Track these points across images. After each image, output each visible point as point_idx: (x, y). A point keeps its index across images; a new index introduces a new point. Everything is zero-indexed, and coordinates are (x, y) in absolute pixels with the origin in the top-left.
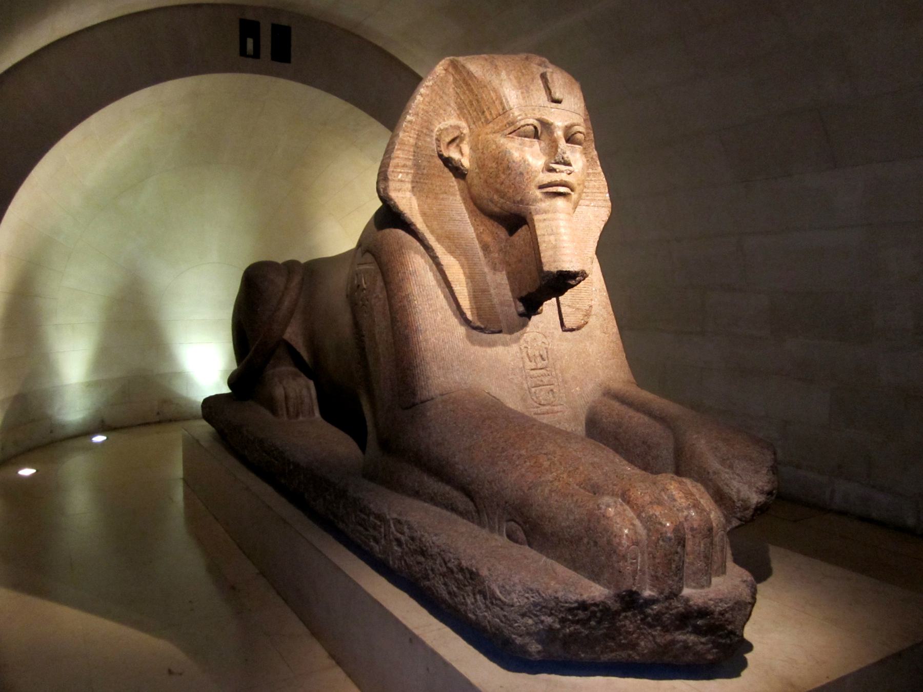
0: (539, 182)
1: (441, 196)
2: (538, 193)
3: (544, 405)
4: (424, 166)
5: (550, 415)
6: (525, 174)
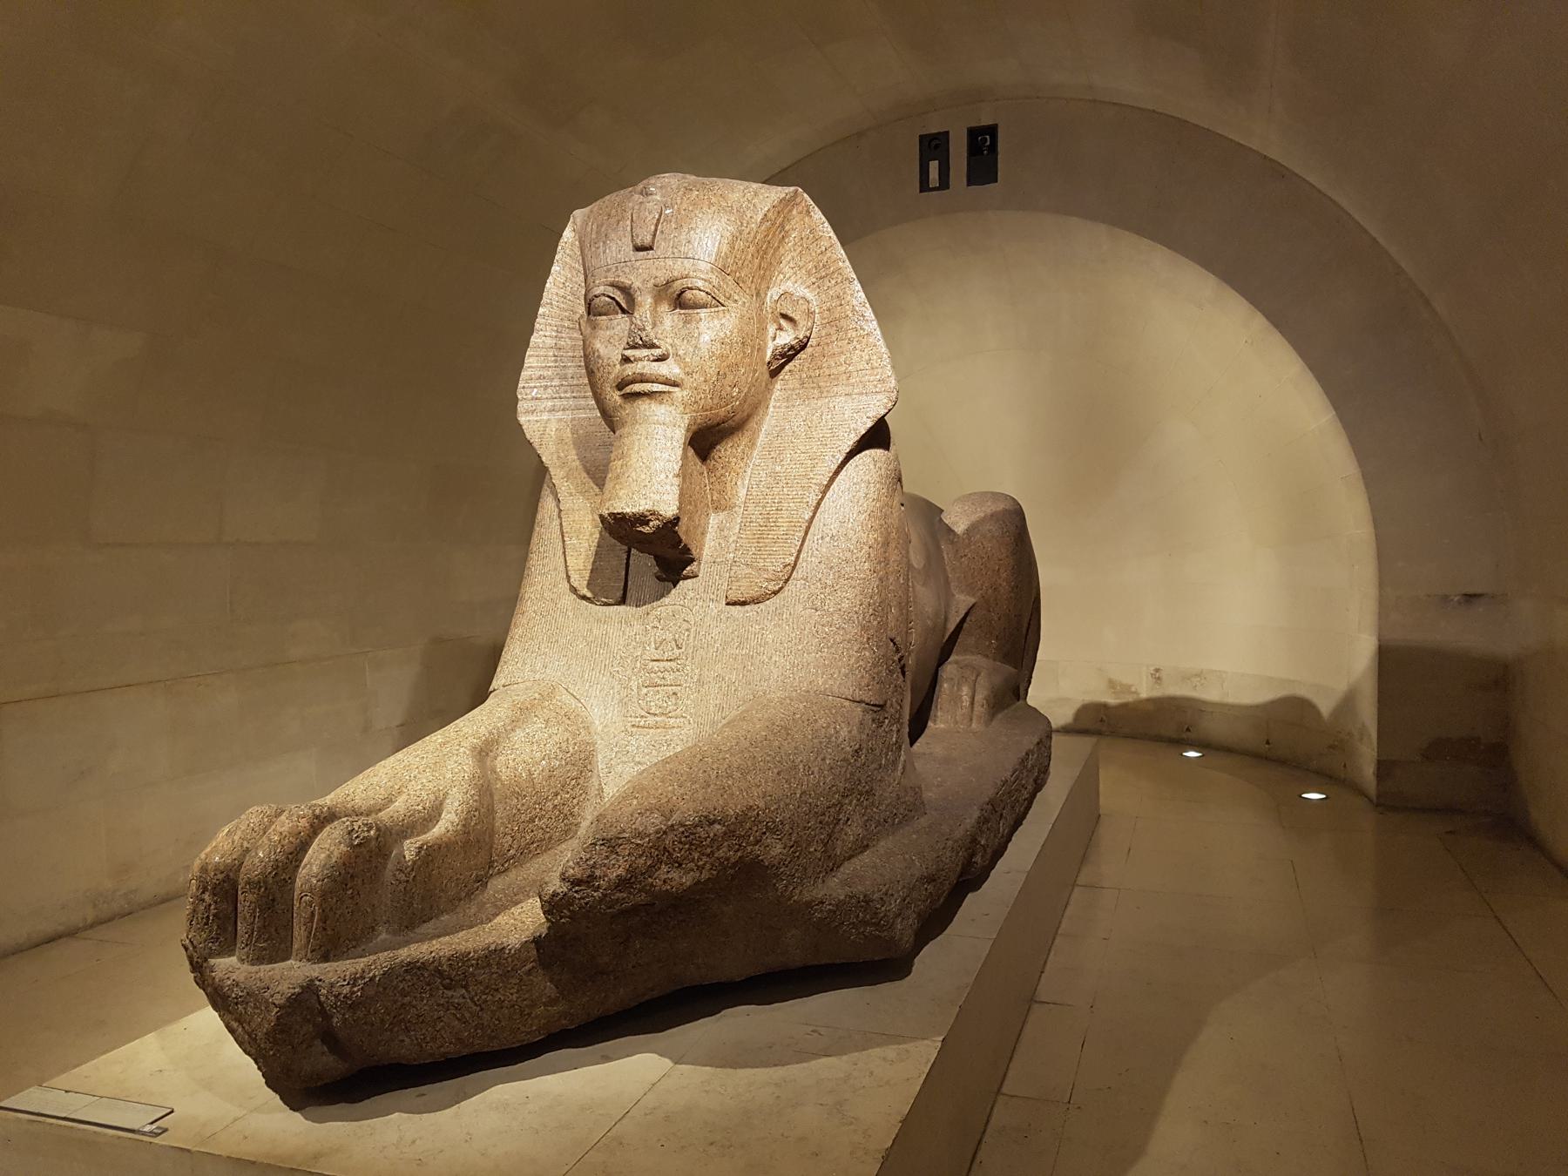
0: (615, 382)
2: (615, 397)
3: (655, 715)
5: (659, 731)
6: (595, 371)
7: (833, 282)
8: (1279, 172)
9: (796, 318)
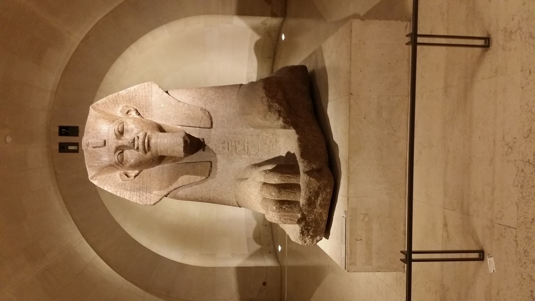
1: (152, 177)
2: (149, 154)
3: (244, 147)
4: (139, 186)
6: (140, 160)
7: (118, 99)
8: (87, 37)
9: (128, 110)
